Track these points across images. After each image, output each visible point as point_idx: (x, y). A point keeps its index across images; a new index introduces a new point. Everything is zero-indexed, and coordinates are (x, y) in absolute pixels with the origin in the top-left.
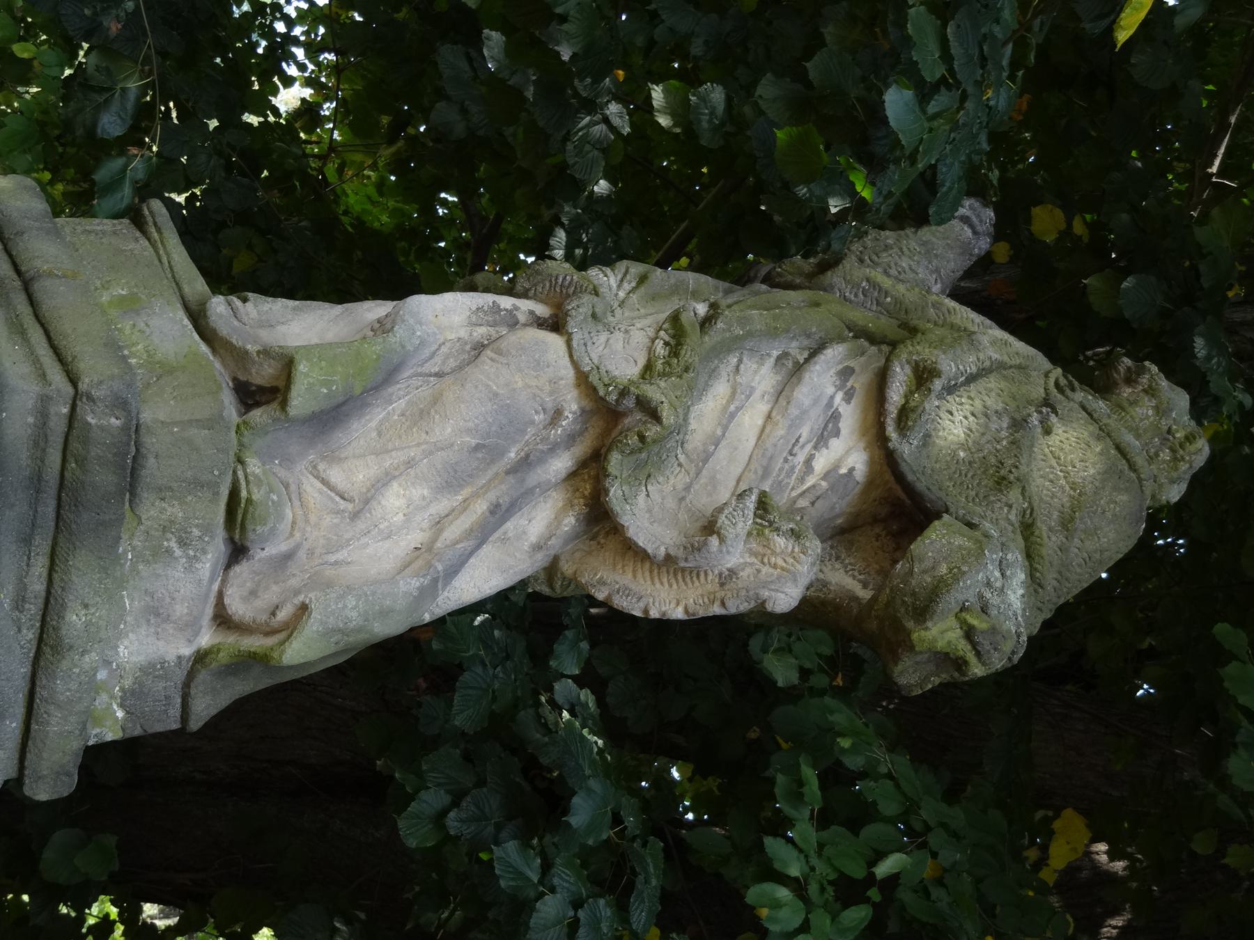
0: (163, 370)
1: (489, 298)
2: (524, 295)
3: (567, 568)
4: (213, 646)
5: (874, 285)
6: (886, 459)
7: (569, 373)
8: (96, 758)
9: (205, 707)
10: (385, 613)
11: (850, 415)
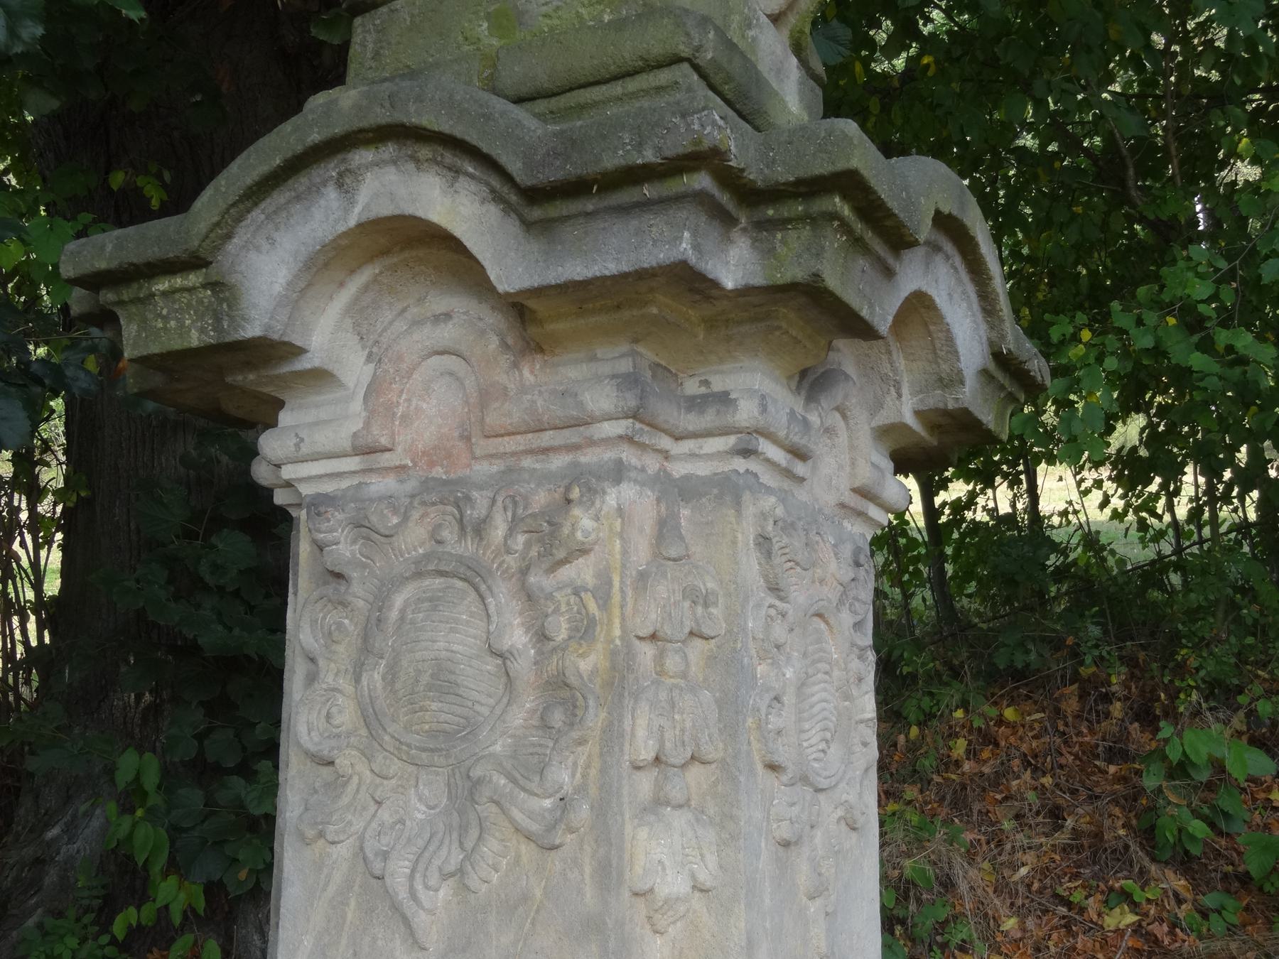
4: (791, 37)
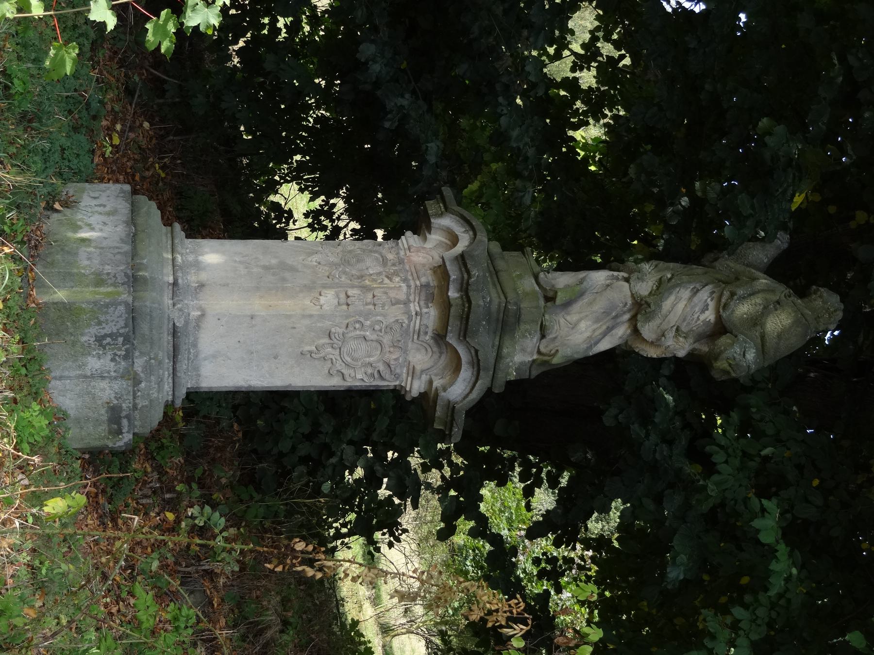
0: (526, 294)
1: (612, 273)
2: (622, 271)
3: (630, 343)
5: (728, 266)
6: (719, 318)
7: (629, 294)
8: (509, 383)
9: (535, 373)
10: (577, 353)
11: (712, 305)
